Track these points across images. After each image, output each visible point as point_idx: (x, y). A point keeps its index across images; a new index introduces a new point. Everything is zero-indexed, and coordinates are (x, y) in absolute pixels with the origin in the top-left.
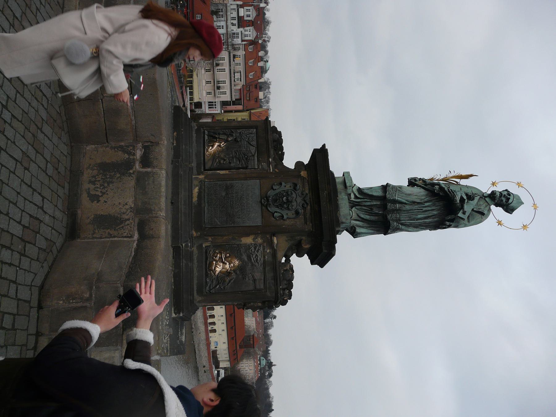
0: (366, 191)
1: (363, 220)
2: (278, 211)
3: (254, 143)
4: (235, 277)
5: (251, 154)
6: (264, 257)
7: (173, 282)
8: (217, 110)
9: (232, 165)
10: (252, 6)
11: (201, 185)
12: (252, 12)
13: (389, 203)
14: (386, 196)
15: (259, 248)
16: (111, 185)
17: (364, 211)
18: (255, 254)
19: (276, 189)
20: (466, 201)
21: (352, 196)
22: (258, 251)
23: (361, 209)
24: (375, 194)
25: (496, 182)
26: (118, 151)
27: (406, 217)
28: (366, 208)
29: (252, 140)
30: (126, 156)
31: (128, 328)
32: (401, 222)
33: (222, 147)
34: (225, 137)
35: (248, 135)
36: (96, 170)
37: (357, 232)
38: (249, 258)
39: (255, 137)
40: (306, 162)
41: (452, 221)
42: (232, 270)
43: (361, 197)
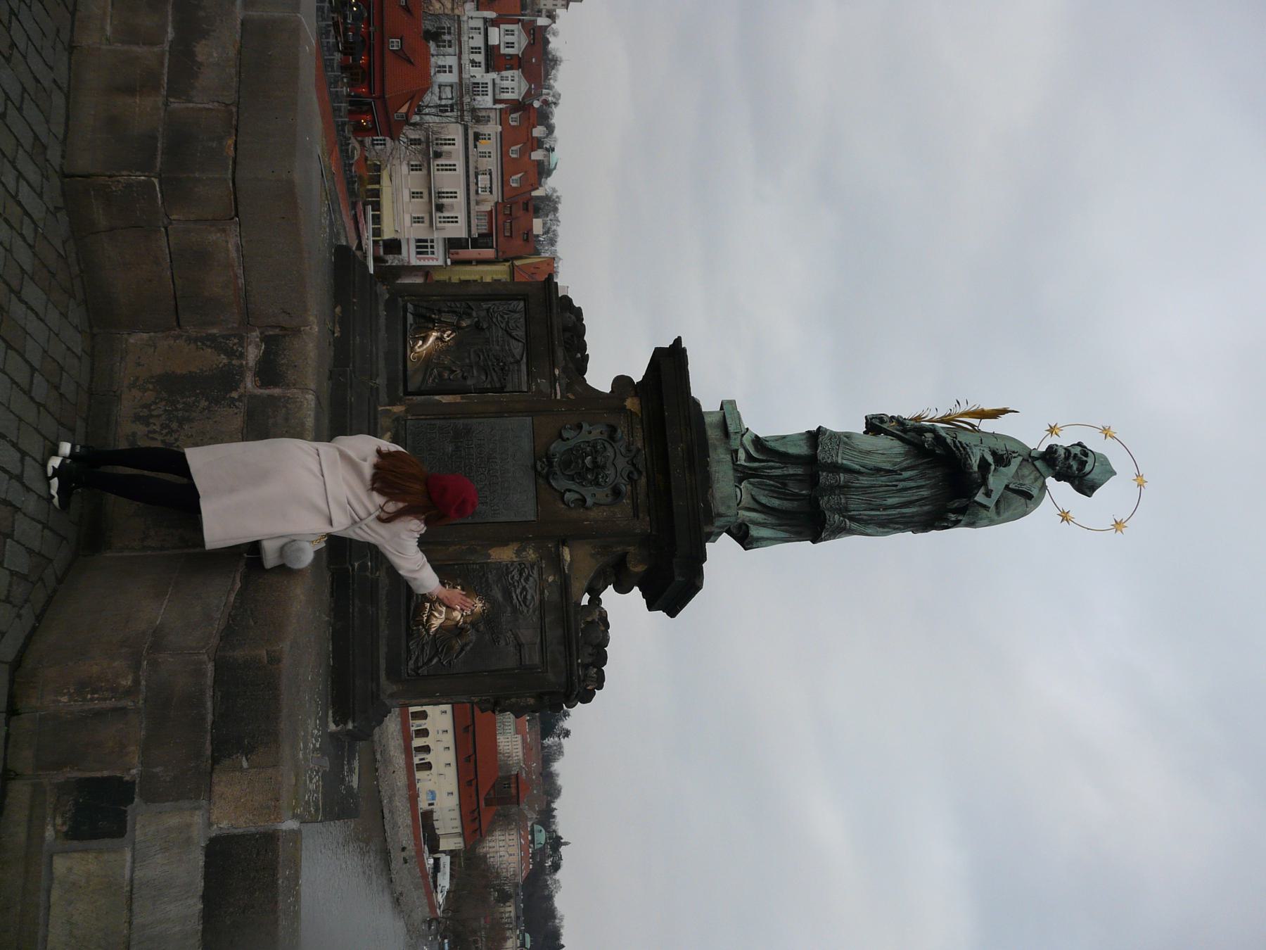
0: (772, 444)
1: (764, 509)
2: (573, 487)
3: (520, 333)
4: (474, 638)
6: (542, 593)
7: (331, 649)
8: (437, 260)
9: (470, 382)
10: (518, 23)
12: (519, 37)
13: (823, 471)
14: (816, 453)
15: (529, 572)
16: (186, 427)
17: (768, 488)
18: (521, 587)
19: (568, 439)
20: (993, 467)
21: (742, 455)
22: (527, 580)
23: (761, 484)
24: (792, 450)
25: (1058, 426)
26: (204, 347)
28: (772, 482)
30: (224, 359)
31: (225, 757)
33: (445, 342)
34: (451, 319)
36: (151, 390)
37: (752, 536)
38: (507, 594)
39: (522, 320)
40: (637, 377)
41: (962, 511)
42: (469, 622)
43: (761, 457)
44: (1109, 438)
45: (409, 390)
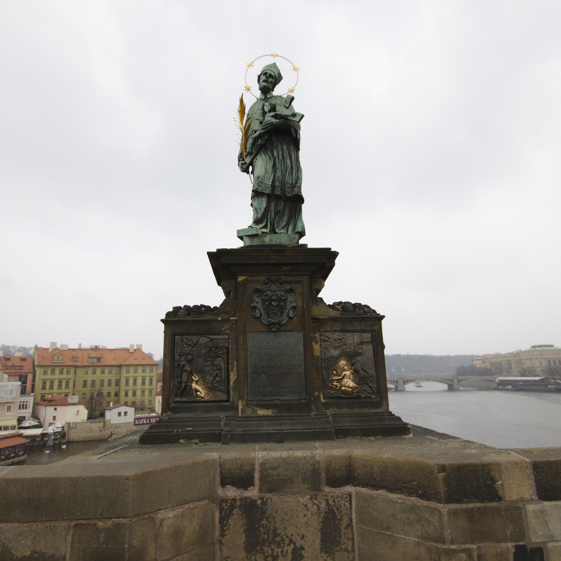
0: (259, 215)
2: (287, 311)
3: (195, 339)
5: (209, 342)
6: (336, 331)
8: (30, 400)
11: (252, 405)
18: (333, 341)
19: (261, 314)
20: (277, 113)
21: (264, 230)
25: (246, 86)
27: (290, 178)
29: (190, 341)
32: (294, 183)
34: (184, 377)
35: (183, 345)
39: (187, 337)
43: (265, 221)
44: (253, 65)
45: (227, 399)
